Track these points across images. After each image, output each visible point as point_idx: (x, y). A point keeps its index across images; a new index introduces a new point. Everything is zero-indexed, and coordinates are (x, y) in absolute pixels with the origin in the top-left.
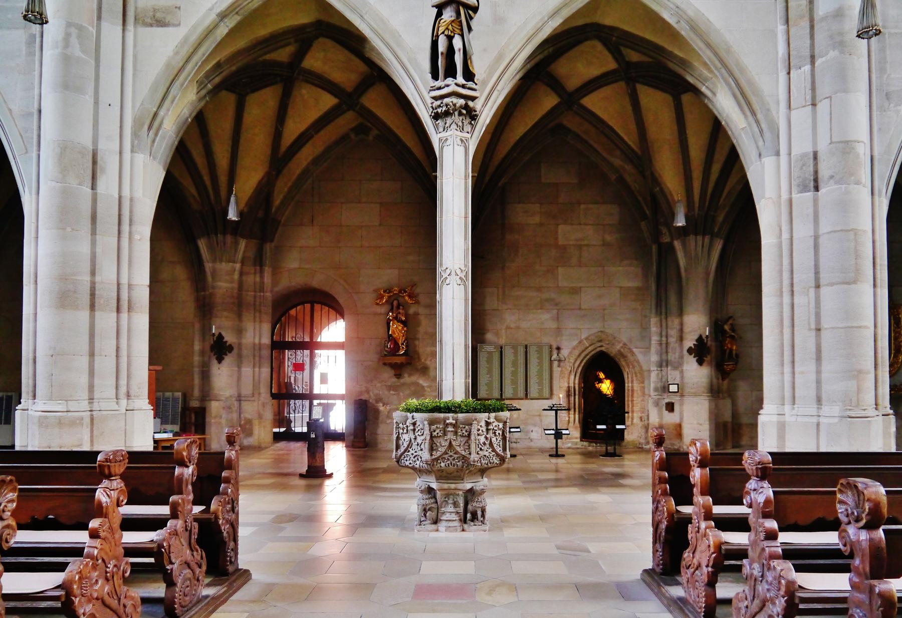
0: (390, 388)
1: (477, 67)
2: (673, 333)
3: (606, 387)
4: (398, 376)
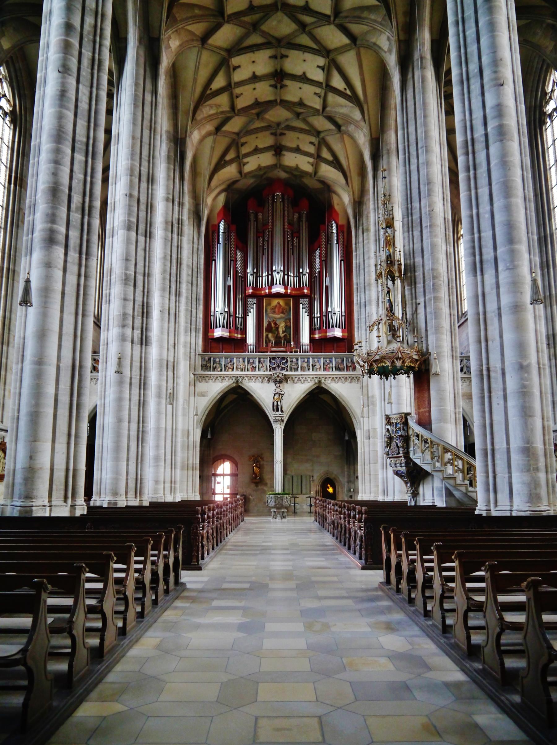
0: (254, 490)
1: (284, 409)
2: (352, 471)
3: (331, 490)
4: (257, 486)
